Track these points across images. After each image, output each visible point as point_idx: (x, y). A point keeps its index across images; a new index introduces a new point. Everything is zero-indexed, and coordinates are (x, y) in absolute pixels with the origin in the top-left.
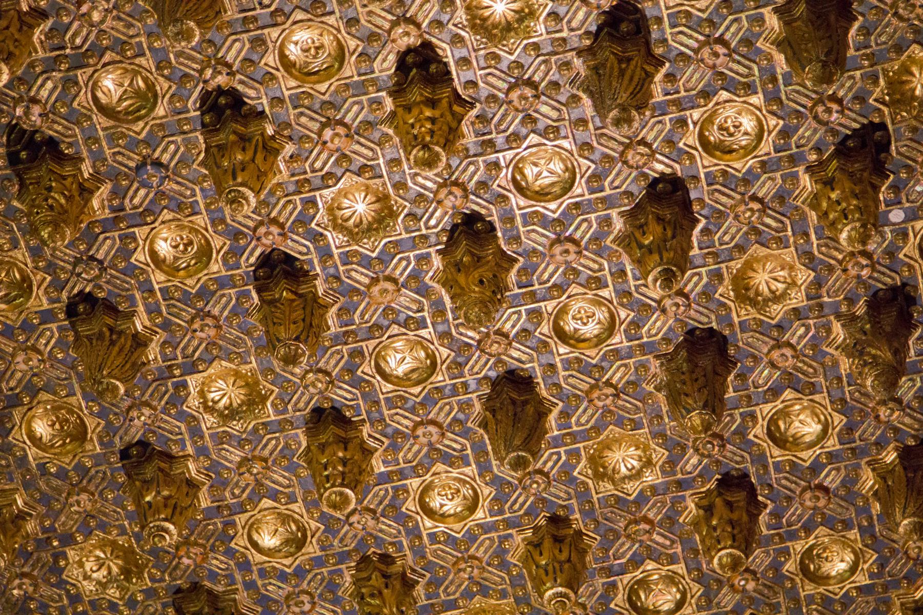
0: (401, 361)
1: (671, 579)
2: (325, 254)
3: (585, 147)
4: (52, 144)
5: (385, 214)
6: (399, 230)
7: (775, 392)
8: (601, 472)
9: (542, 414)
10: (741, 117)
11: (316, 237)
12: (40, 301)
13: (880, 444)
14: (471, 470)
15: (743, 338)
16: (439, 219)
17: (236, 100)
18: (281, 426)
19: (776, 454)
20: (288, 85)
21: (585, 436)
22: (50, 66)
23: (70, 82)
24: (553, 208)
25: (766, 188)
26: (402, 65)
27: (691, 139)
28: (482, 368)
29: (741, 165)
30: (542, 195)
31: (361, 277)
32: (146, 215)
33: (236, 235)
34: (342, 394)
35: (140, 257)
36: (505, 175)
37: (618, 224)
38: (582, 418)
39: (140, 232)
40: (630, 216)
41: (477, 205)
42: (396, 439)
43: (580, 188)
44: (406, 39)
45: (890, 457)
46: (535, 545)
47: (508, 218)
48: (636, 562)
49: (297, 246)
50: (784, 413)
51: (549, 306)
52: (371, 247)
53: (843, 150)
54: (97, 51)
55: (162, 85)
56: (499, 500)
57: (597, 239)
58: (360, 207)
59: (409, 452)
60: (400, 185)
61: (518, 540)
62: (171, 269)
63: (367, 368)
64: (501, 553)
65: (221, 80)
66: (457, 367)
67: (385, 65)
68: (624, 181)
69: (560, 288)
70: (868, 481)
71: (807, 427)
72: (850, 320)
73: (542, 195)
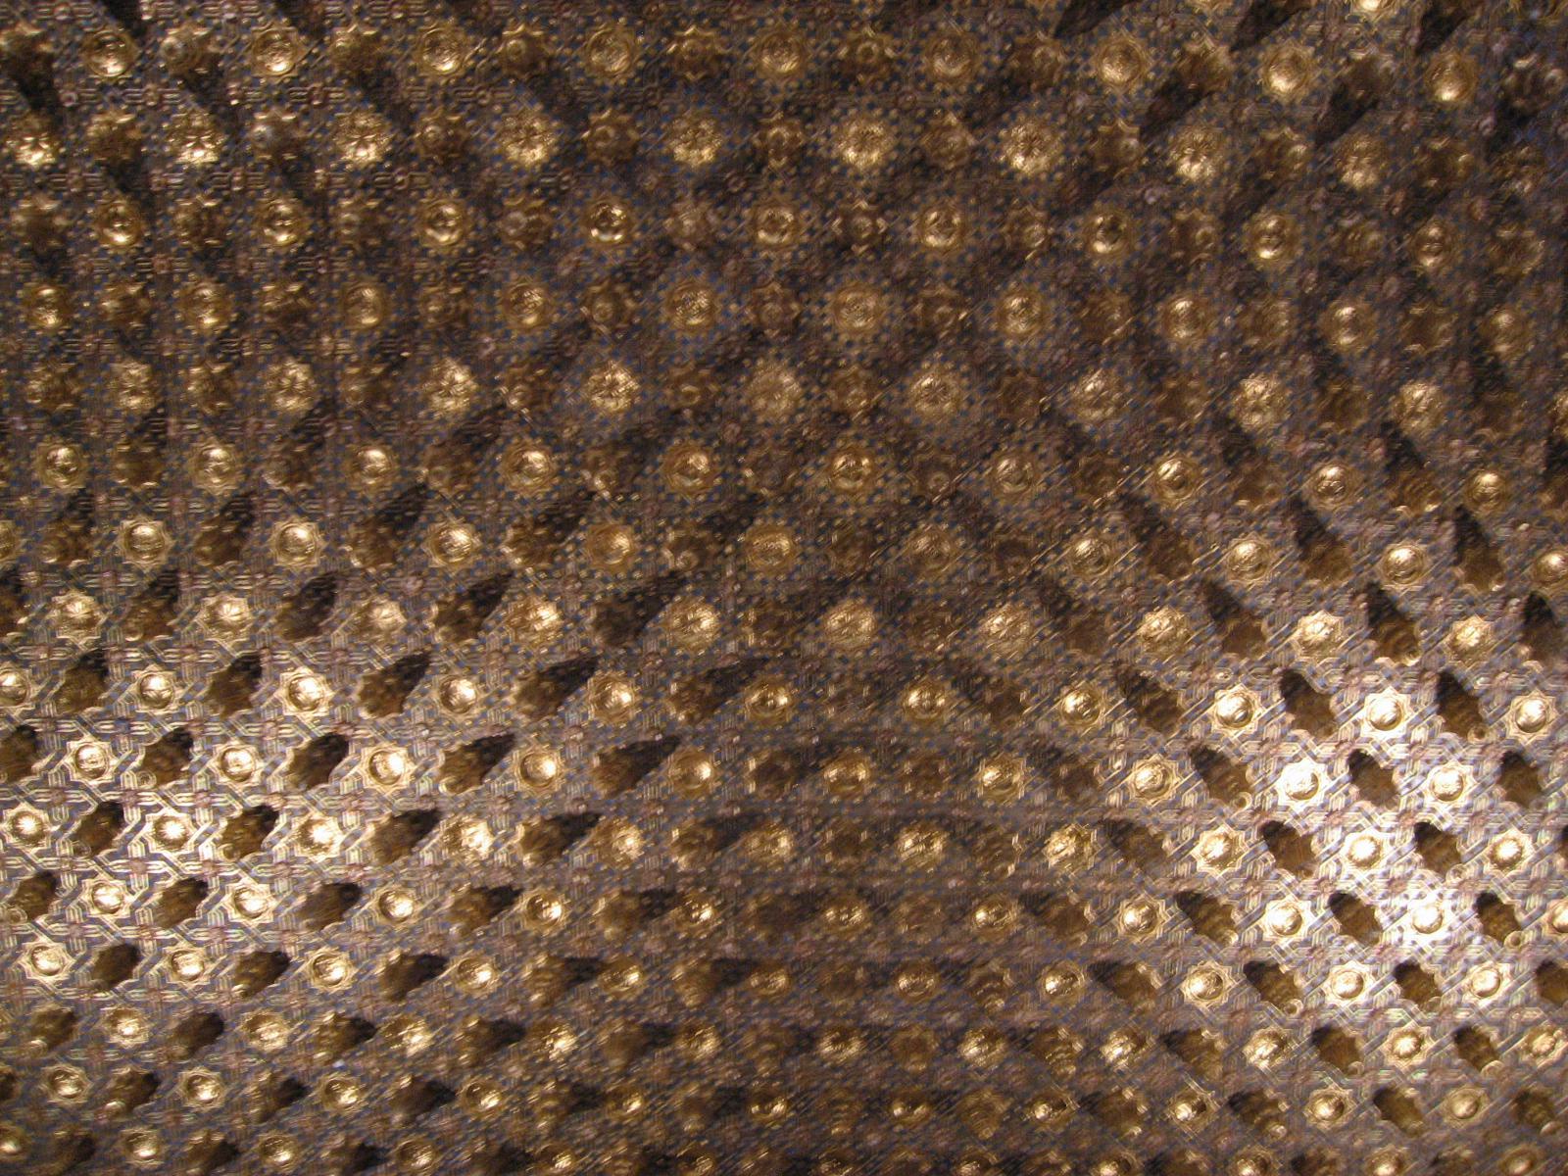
0: (108, 897)
1: (79, 1085)
2: (137, 829)
3: (276, 912)
4: (105, 672)
5: (178, 844)
6: (172, 856)
7: (213, 1069)
8: (114, 1020)
9: (128, 975)
10: (339, 971)
11: (143, 821)
12: (16, 711)
13: (221, 1129)
14: (71, 961)
15: (229, 1038)
16: (191, 869)
17: (189, 744)
18: (30, 862)
19: (180, 1089)
20: (213, 764)
21: (128, 1001)
22: (147, 650)
23: (143, 665)
24: (235, 916)
25: (313, 1001)
26: (261, 808)
27: (314, 955)
28: (130, 934)
29: (315, 984)
30: (240, 908)
31: (137, 851)
32: (99, 736)
33: (117, 782)
34: (68, 881)
35: (73, 745)
36: (237, 886)
37: (249, 950)
38: (136, 994)
39: (87, 737)
40: (259, 954)
41: (214, 883)
42: (60, 918)
43: (255, 922)
44: (275, 803)
45: (218, 1138)
46: (51, 1016)
47: (217, 899)
48: (77, 1064)
49: (132, 816)
50: (205, 1079)
51: (183, 945)
52: (155, 847)
53: (354, 1021)
54: (168, 667)
55: (173, 707)
56: (65, 984)
57: (236, 945)
58: (173, 831)
59: (58, 928)
60: (198, 842)
61: (50, 1006)
62: (78, 762)
63: (89, 882)
64: (35, 1002)
65: (195, 731)
66: (121, 923)
67: (254, 801)
68: (270, 938)
69: (199, 944)
70: (198, 1138)
71: (206, 1093)
72: (273, 1078)
73: (240, 908)
